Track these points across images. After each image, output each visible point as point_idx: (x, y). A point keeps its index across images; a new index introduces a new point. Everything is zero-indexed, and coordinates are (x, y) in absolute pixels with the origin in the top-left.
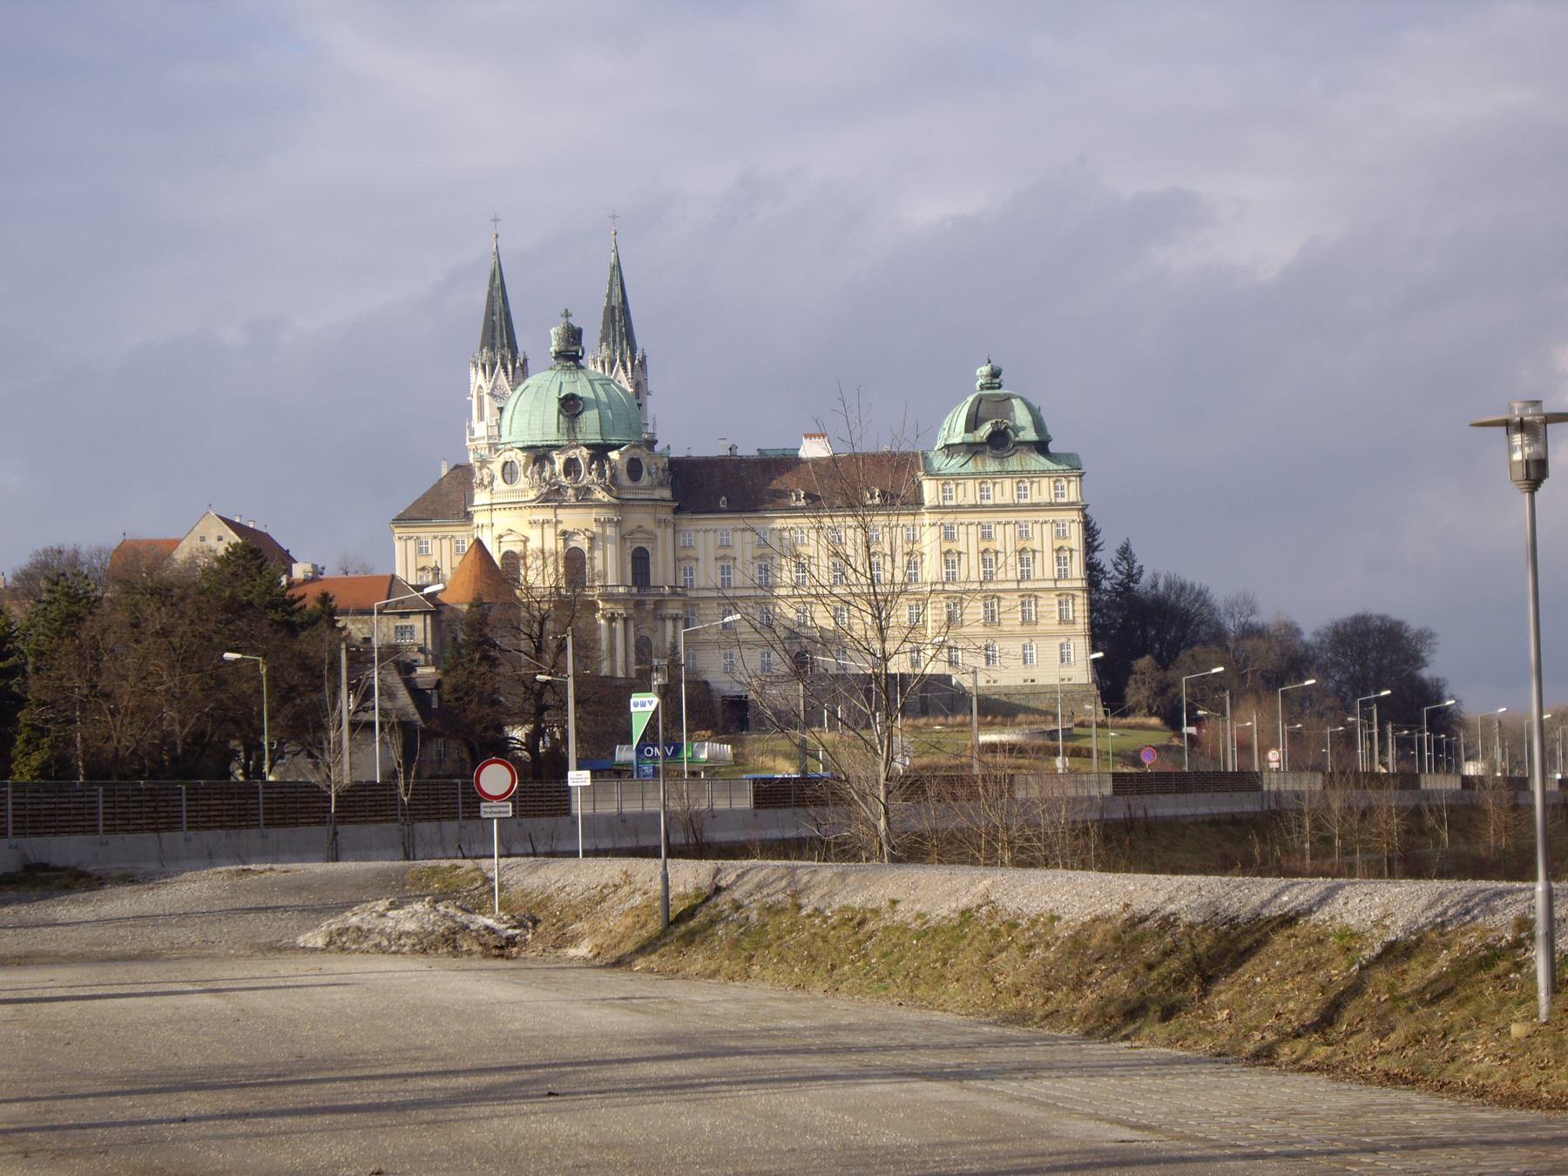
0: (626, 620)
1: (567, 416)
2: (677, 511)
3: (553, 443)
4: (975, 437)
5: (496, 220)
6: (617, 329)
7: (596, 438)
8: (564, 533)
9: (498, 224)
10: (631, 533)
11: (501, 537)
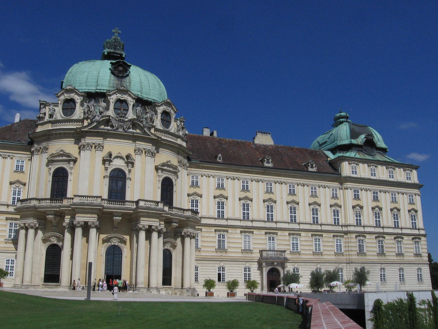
4: (357, 141)
8: (110, 155)
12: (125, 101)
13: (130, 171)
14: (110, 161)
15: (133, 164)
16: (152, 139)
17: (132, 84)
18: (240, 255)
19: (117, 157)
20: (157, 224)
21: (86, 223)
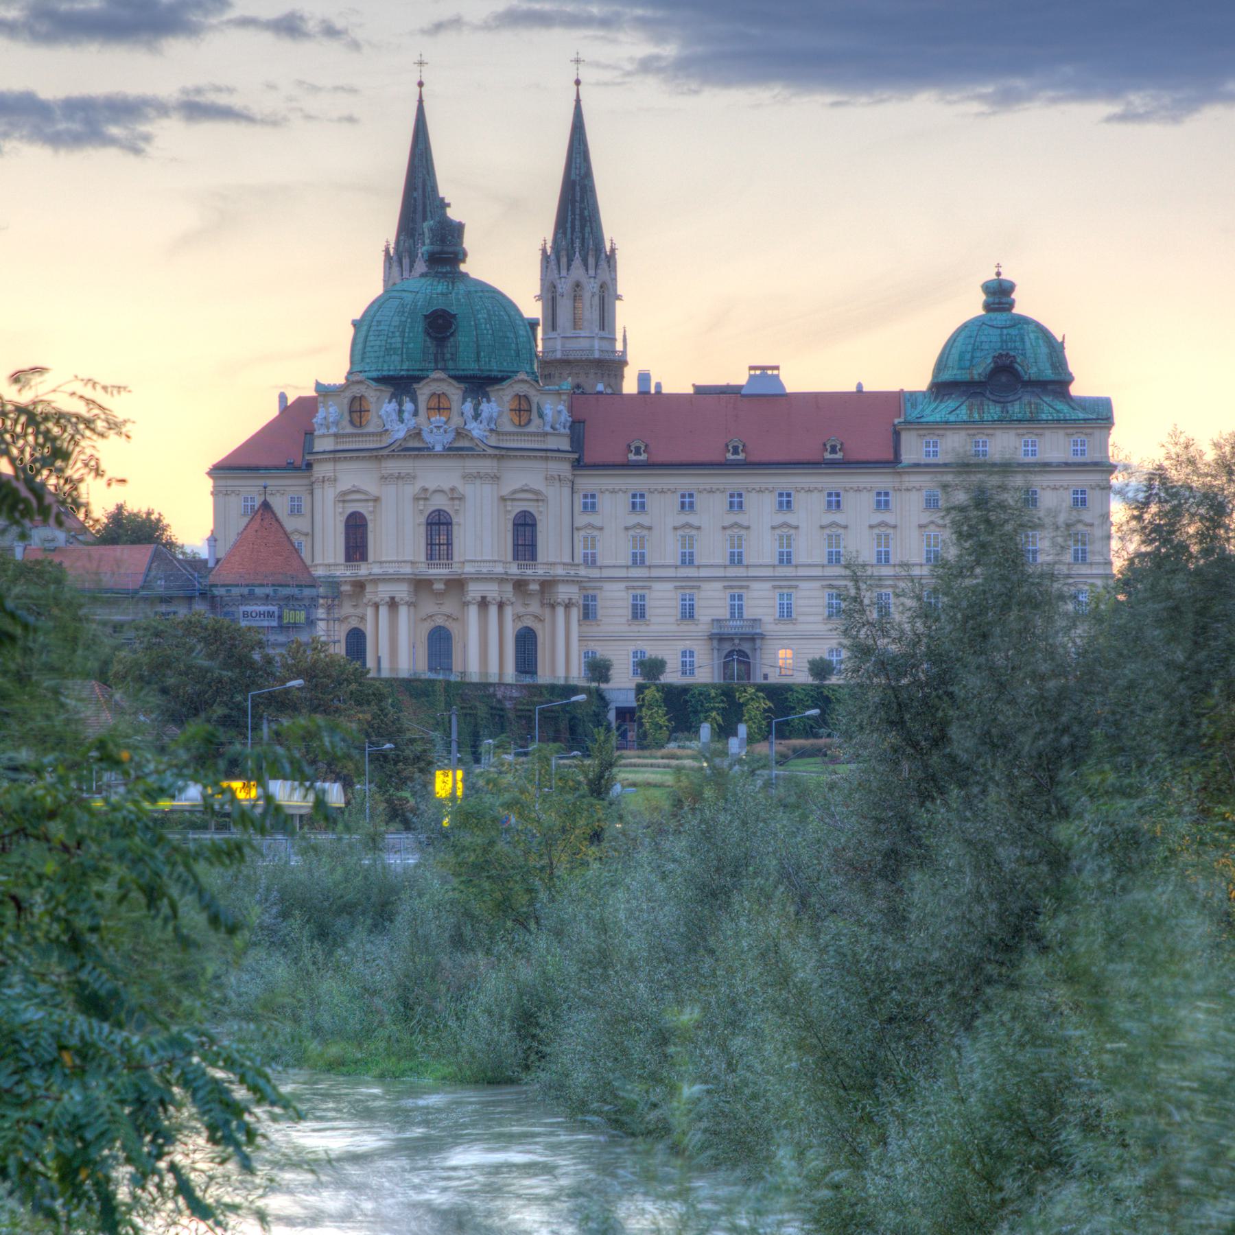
0: (501, 606)
1: (435, 339)
2: (578, 465)
3: (417, 373)
5: (421, 63)
6: (578, 211)
7: (472, 367)
8: (425, 490)
9: (424, 68)
10: (514, 492)
11: (345, 493)
18: (674, 628)
19: (436, 491)
20: (496, 595)
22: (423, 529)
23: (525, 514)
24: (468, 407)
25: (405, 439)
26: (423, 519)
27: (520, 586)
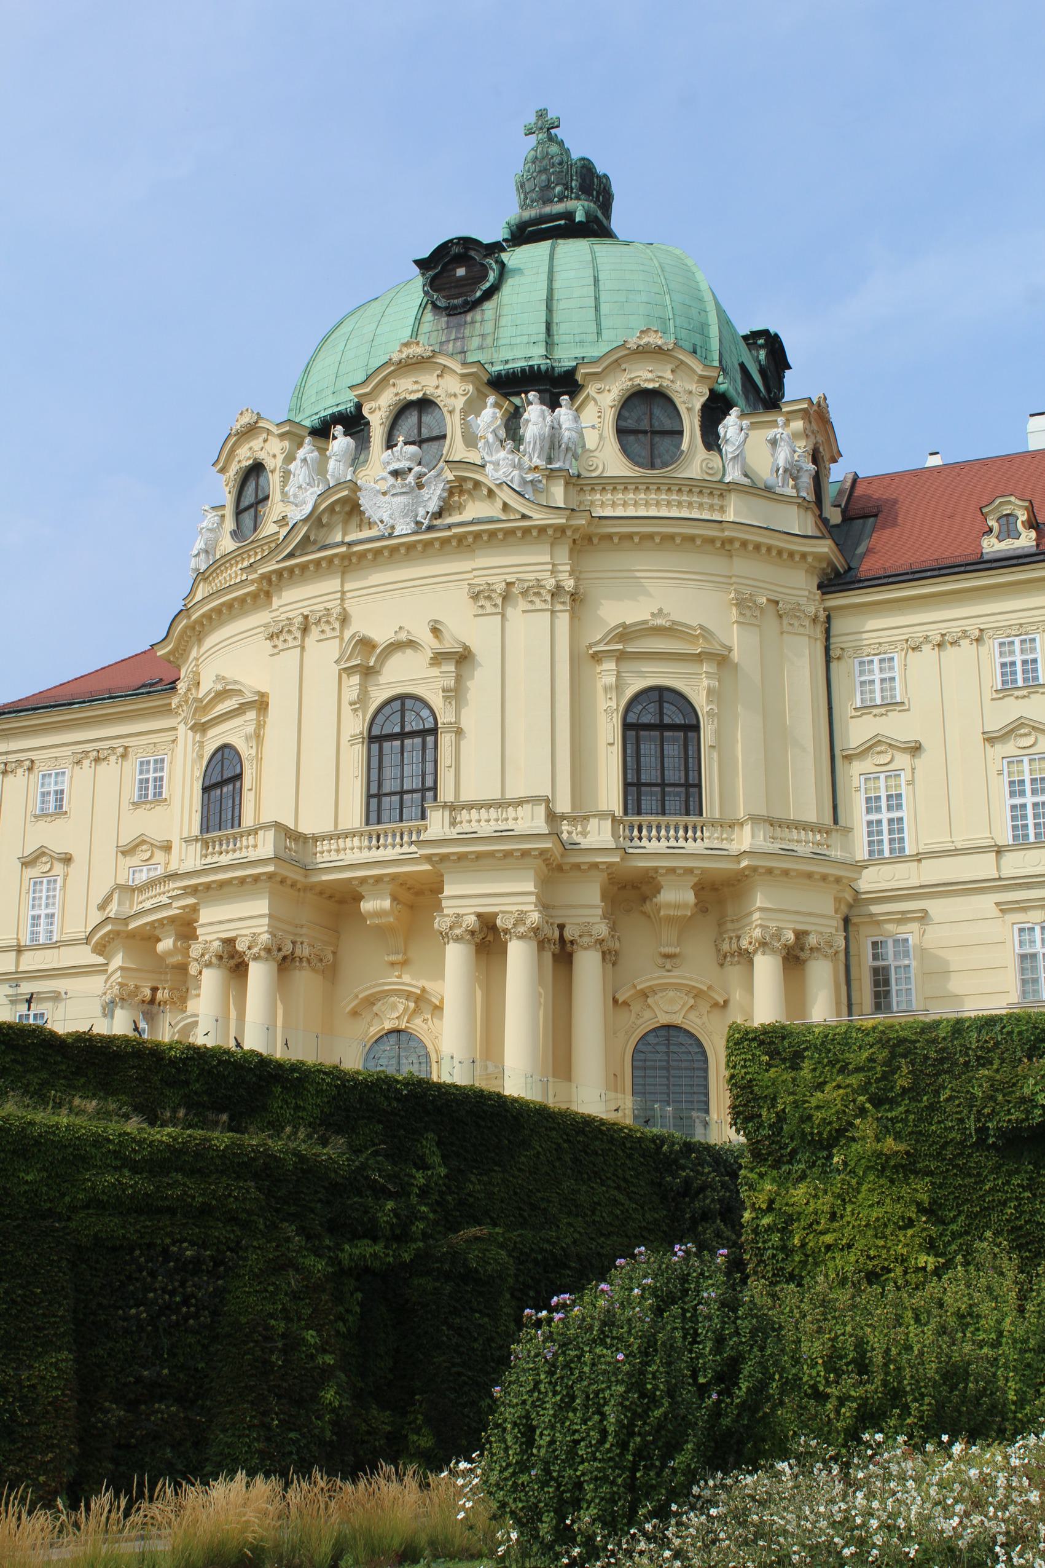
1: (451, 311)
8: (365, 644)
10: (625, 633)
11: (203, 707)
12: (425, 404)
13: (456, 694)
14: (368, 672)
15: (463, 658)
16: (542, 529)
17: (503, 321)
21: (230, 942)
22: (355, 757)
23: (660, 695)
24: (490, 416)
25: (316, 520)
26: (356, 725)
27: (644, 899)
